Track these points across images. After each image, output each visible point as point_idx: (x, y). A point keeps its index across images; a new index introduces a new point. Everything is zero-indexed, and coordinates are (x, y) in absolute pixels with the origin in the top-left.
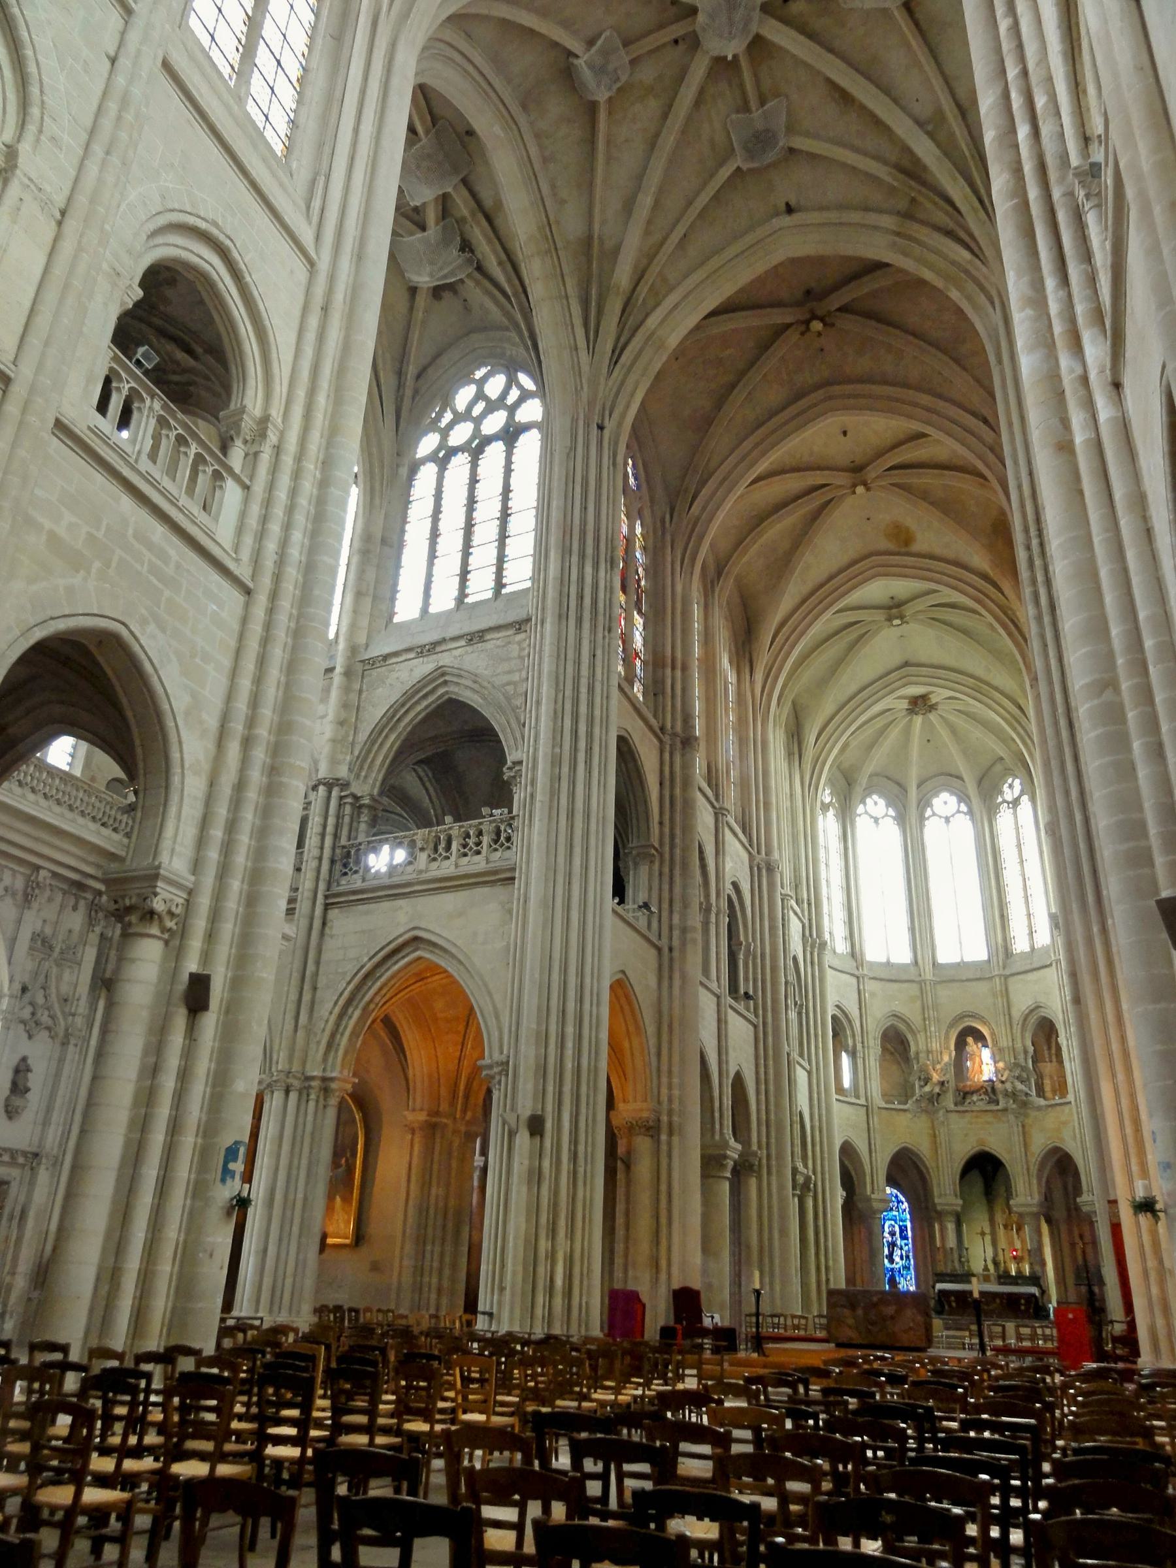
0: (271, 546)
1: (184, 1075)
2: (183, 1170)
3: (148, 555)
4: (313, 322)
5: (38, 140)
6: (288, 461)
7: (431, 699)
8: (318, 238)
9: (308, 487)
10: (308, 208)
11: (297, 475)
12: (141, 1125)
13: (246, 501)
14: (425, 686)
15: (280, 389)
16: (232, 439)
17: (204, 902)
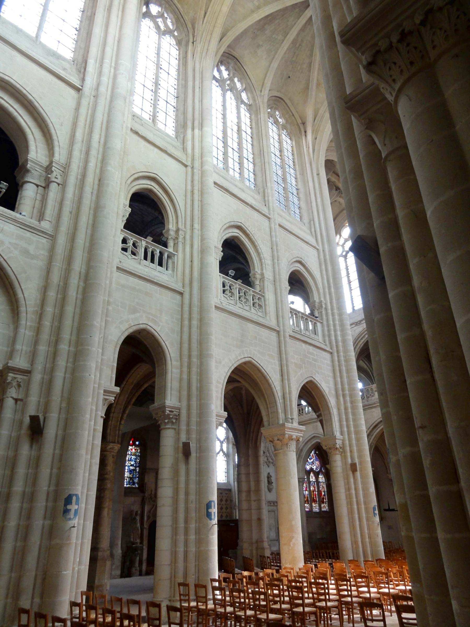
0: (333, 338)
1: (356, 489)
2: (364, 515)
3: (311, 356)
4: (323, 267)
5: (266, 267)
6: (330, 311)
7: (364, 339)
8: (317, 240)
9: (337, 317)
10: (311, 232)
11: (333, 315)
12: (350, 503)
13: (323, 326)
14: (361, 335)
15: (321, 291)
16: (314, 310)
17: (347, 442)
